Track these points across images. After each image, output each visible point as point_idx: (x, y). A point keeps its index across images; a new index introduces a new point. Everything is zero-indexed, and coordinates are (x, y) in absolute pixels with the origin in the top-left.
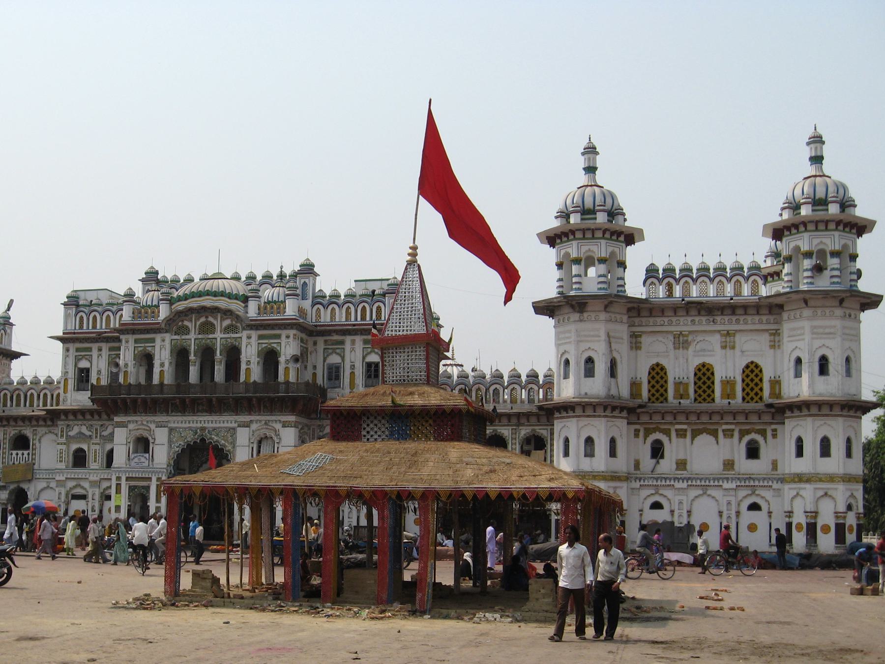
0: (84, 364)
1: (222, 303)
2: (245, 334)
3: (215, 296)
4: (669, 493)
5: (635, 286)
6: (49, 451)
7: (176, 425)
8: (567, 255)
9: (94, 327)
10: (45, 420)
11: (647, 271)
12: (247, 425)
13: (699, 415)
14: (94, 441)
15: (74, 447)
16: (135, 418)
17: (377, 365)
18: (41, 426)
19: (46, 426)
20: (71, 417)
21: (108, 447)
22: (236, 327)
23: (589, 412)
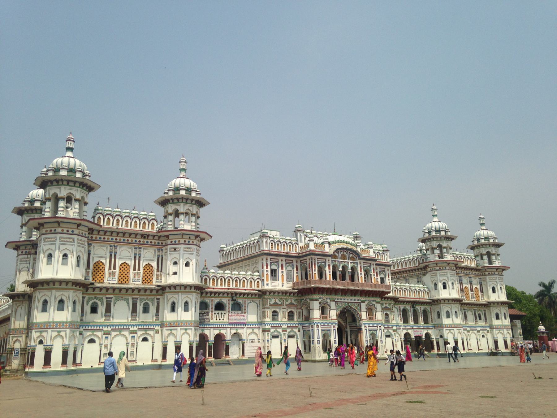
2: (359, 261)
9: (278, 249)
10: (252, 294)
15: (273, 310)
16: (322, 296)
19: (251, 298)
20: (272, 294)
21: (289, 310)
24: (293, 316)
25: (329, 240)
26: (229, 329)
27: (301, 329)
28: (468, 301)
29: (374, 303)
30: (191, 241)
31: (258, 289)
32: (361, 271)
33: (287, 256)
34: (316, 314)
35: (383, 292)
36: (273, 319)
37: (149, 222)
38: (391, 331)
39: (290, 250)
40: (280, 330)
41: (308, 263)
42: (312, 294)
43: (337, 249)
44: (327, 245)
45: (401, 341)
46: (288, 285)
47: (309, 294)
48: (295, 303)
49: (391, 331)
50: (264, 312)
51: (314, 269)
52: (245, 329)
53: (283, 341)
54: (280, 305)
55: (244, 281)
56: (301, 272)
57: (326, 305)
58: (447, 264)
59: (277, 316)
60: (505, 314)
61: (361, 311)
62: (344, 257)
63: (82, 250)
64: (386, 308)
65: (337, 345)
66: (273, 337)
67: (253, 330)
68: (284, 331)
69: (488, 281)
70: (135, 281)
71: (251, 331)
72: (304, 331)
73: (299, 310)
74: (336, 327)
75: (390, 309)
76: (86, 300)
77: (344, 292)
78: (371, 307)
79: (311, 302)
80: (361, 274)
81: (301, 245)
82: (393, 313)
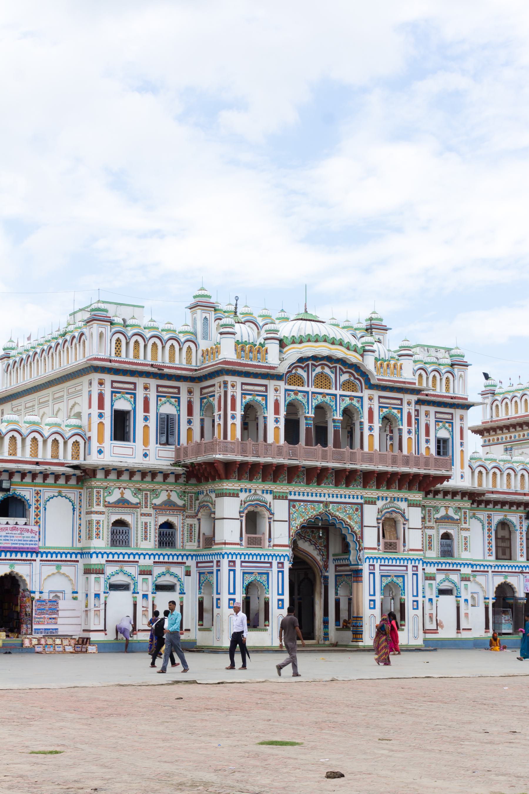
0: (123, 405)
2: (366, 393)
3: (333, 343)
6: (56, 520)
7: (297, 497)
9: (136, 356)
10: (57, 477)
12: (373, 502)
14: (144, 510)
15: (114, 518)
16: (249, 486)
17: (445, 441)
18: (49, 486)
20: (113, 476)
21: (162, 520)
22: (354, 385)
24: (173, 535)
25: (280, 335)
27: (194, 571)
29: (403, 505)
31: (75, 462)
32: (371, 420)
33: (159, 374)
34: (230, 531)
35: (426, 477)
36: (114, 543)
38: (455, 577)
39: (172, 358)
40: (133, 570)
41: (217, 396)
42: (220, 478)
43: (301, 360)
44: (273, 348)
45: (487, 608)
46: (162, 454)
47: (214, 479)
48: (180, 503)
50: (90, 522)
51: (229, 412)
52: (37, 564)
53: (139, 597)
54: (136, 506)
55: (34, 439)
56: (202, 420)
57: (259, 509)
59: (127, 533)
61: (362, 526)
62: (322, 380)
64: (447, 519)
65: (284, 612)
66: (114, 587)
67: (58, 567)
68: (146, 572)
71: (52, 569)
72: (200, 574)
73: (189, 521)
74: (287, 565)
77: (316, 476)
78: (394, 515)
79: (218, 500)
80: (371, 429)
81: (204, 345)
82: (464, 534)
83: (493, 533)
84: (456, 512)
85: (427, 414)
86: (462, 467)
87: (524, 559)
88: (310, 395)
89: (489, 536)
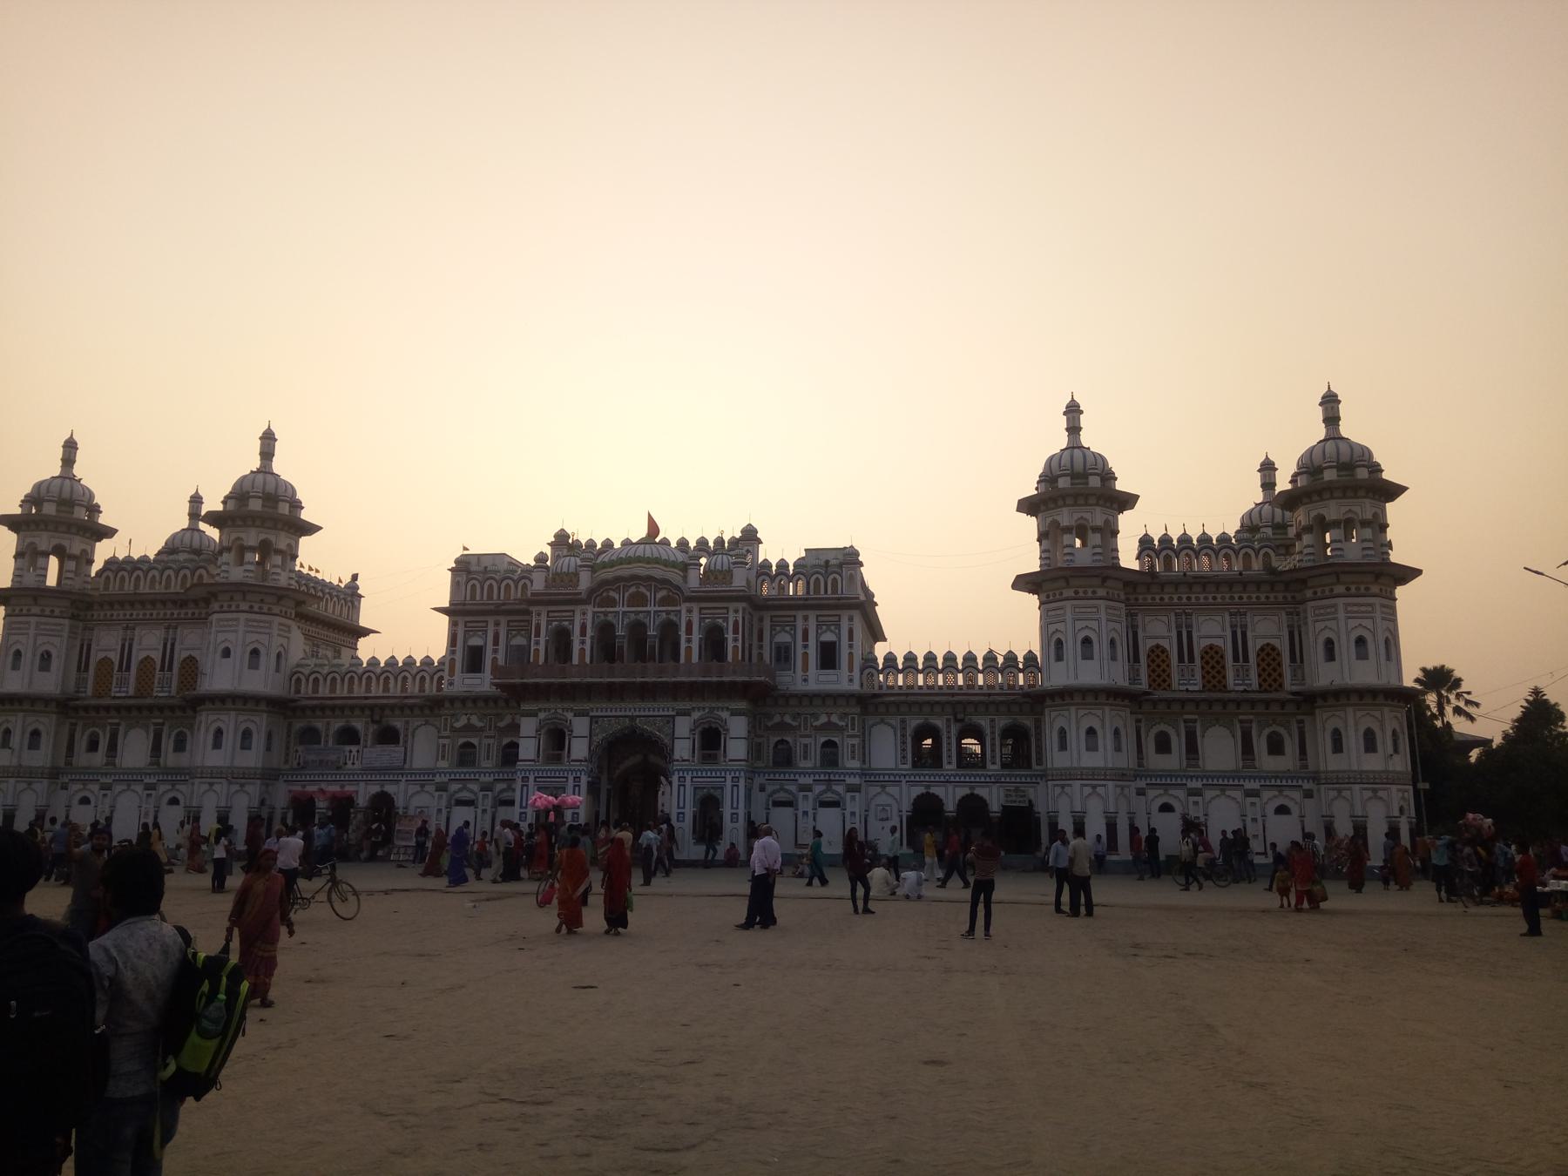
0: (476, 641)
1: (658, 572)
2: (684, 607)
4: (1181, 793)
5: (1128, 557)
6: (425, 747)
8: (1055, 524)
9: (490, 597)
10: (422, 708)
11: (1141, 541)
12: (686, 713)
13: (1210, 703)
15: (461, 741)
16: (546, 706)
17: (834, 643)
20: (458, 704)
21: (506, 741)
23: (1090, 699)
26: (362, 784)
28: (1203, 696)
29: (725, 715)
30: (234, 605)
33: (497, 611)
37: (193, 575)
38: (840, 789)
40: (475, 787)
49: (840, 789)
52: (402, 785)
54: (482, 729)
58: (1062, 583)
60: (1394, 732)
61: (673, 739)
63: (56, 641)
64: (829, 726)
66: (460, 803)
67: (422, 786)
68: (486, 788)
69: (1310, 620)
70: (166, 689)
74: (584, 780)
75: (841, 729)
76: (79, 729)
77: (613, 692)
80: (689, 641)
83: (909, 740)
84: (841, 718)
85: (806, 618)
86: (851, 669)
87: (954, 766)
88: (621, 614)
89: (904, 743)
